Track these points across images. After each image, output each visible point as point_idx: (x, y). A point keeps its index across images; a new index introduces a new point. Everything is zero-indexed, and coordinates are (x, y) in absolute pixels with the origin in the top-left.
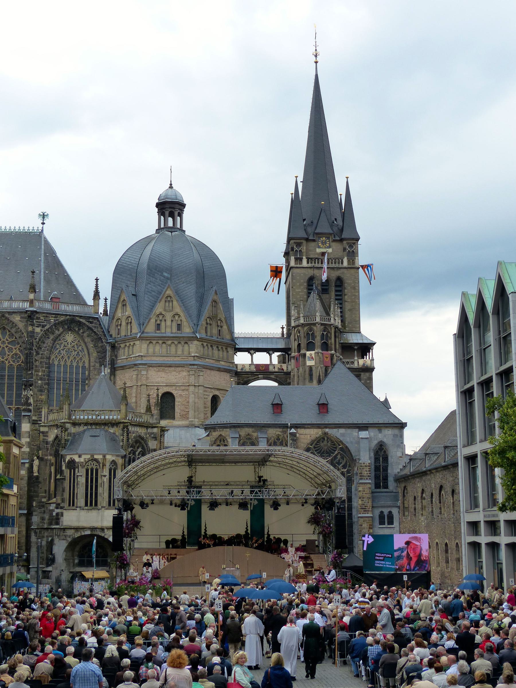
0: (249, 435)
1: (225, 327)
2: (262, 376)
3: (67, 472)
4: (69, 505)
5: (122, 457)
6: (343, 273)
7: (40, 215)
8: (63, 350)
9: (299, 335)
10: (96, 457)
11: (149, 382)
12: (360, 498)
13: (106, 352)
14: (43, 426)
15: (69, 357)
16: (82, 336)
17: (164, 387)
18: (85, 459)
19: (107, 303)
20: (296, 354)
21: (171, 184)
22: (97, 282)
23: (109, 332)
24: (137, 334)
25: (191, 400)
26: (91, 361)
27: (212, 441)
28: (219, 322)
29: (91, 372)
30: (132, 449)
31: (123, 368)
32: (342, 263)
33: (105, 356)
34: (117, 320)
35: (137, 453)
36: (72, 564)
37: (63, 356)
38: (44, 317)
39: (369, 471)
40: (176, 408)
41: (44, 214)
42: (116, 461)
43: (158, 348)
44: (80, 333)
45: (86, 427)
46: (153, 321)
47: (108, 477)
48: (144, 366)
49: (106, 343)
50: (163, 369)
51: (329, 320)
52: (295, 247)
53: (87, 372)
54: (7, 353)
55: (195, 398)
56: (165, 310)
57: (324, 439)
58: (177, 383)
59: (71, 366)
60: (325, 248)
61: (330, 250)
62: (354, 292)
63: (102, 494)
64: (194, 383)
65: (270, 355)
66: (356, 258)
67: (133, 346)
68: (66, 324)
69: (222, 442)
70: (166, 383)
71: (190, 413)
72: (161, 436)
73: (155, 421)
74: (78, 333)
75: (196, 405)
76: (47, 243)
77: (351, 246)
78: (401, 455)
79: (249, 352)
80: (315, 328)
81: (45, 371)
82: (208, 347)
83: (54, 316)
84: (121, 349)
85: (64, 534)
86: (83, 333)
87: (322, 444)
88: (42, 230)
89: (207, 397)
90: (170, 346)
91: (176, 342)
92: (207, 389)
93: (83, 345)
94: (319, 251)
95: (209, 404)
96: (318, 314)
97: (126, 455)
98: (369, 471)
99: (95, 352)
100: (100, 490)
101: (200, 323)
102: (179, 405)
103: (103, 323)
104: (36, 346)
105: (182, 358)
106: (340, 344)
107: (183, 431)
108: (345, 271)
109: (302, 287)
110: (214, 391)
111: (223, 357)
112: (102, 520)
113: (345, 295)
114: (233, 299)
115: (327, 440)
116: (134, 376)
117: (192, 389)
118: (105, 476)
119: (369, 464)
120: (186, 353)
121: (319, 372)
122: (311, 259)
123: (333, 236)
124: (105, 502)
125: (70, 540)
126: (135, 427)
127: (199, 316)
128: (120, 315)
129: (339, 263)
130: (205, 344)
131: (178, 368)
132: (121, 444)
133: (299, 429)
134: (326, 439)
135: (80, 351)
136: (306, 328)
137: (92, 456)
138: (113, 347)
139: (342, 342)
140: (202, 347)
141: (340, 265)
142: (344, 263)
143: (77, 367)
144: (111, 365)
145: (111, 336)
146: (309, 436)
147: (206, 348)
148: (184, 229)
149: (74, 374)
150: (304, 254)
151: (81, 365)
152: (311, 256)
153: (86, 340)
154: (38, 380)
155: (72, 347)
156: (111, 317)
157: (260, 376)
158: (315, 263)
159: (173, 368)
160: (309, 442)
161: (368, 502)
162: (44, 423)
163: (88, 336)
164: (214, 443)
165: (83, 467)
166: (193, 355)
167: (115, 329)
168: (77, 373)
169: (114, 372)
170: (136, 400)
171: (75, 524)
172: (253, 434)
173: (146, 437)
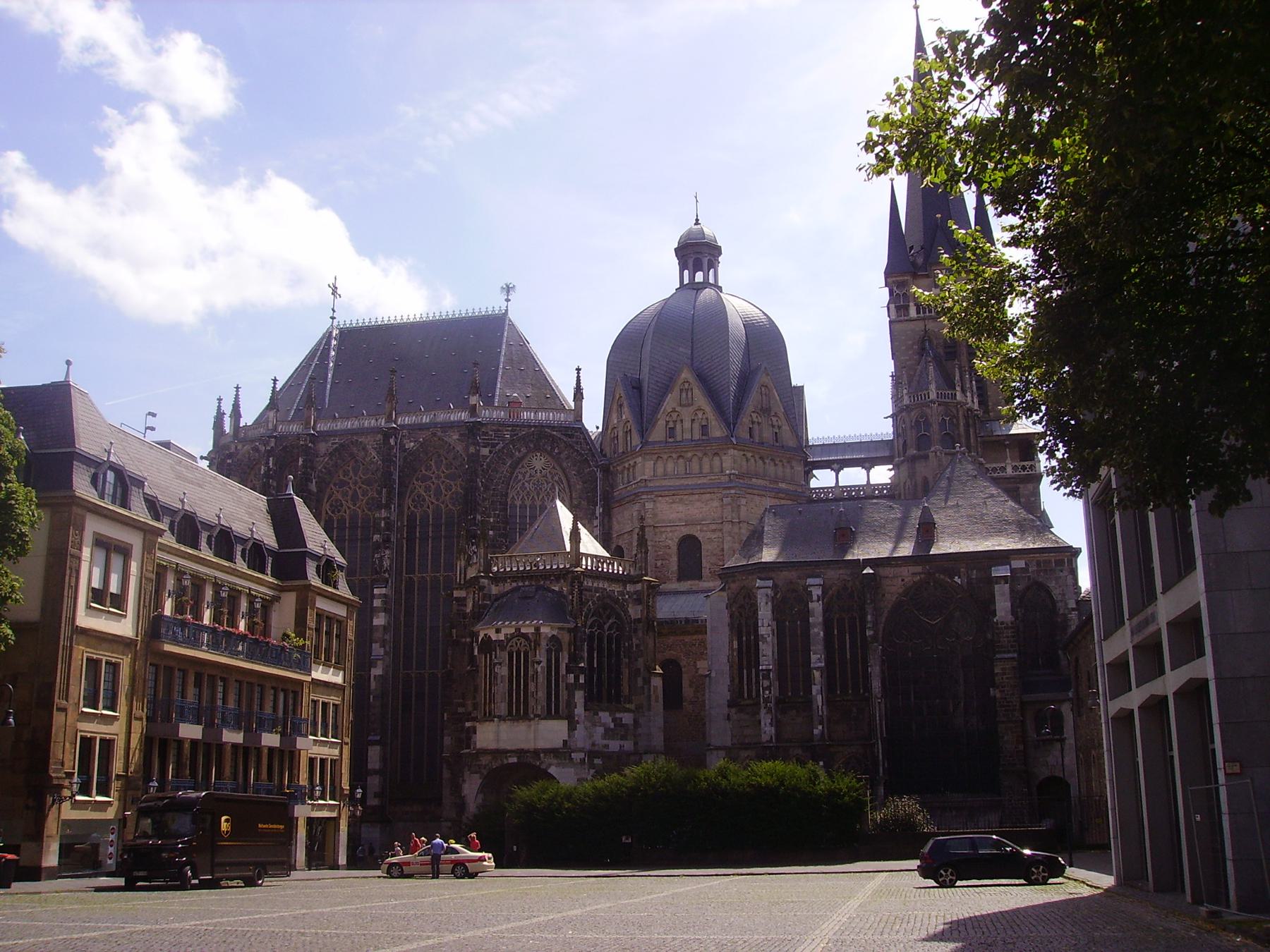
3: (482, 661)
4: (485, 714)
5: (569, 630)
7: (502, 288)
8: (529, 482)
10: (523, 631)
14: (457, 589)
15: (538, 495)
17: (682, 528)
18: (506, 635)
21: (697, 220)
22: (578, 373)
24: (637, 446)
25: (726, 547)
28: (774, 419)
34: (613, 429)
35: (606, 627)
38: (494, 431)
40: (704, 561)
41: (508, 286)
42: (560, 636)
43: (670, 466)
45: (514, 584)
46: (661, 423)
47: (544, 664)
52: (895, 288)
54: (443, 491)
57: (929, 583)
65: (868, 470)
67: (634, 466)
68: (532, 441)
70: (686, 521)
72: (648, 595)
73: (638, 572)
74: (550, 454)
76: (512, 325)
78: (1074, 606)
80: (928, 411)
81: (499, 515)
82: (755, 461)
83: (510, 429)
85: (478, 763)
86: (560, 453)
88: (507, 311)
96: (933, 387)
97: (576, 626)
100: (532, 687)
101: (739, 420)
104: (485, 477)
106: (979, 439)
112: (535, 739)
117: (727, 527)
118: (539, 663)
120: (716, 470)
124: (539, 707)
125: (485, 772)
128: (616, 422)
130: (749, 455)
131: (703, 496)
132: (570, 608)
136: (913, 414)
137: (518, 630)
138: (606, 470)
139: (982, 434)
145: (605, 456)
146: (900, 579)
147: (752, 460)
148: (720, 285)
153: (565, 464)
154: (489, 530)
160: (901, 591)
162: (460, 584)
163: (567, 458)
164: (734, 602)
165: (503, 648)
166: (728, 472)
171: (493, 746)
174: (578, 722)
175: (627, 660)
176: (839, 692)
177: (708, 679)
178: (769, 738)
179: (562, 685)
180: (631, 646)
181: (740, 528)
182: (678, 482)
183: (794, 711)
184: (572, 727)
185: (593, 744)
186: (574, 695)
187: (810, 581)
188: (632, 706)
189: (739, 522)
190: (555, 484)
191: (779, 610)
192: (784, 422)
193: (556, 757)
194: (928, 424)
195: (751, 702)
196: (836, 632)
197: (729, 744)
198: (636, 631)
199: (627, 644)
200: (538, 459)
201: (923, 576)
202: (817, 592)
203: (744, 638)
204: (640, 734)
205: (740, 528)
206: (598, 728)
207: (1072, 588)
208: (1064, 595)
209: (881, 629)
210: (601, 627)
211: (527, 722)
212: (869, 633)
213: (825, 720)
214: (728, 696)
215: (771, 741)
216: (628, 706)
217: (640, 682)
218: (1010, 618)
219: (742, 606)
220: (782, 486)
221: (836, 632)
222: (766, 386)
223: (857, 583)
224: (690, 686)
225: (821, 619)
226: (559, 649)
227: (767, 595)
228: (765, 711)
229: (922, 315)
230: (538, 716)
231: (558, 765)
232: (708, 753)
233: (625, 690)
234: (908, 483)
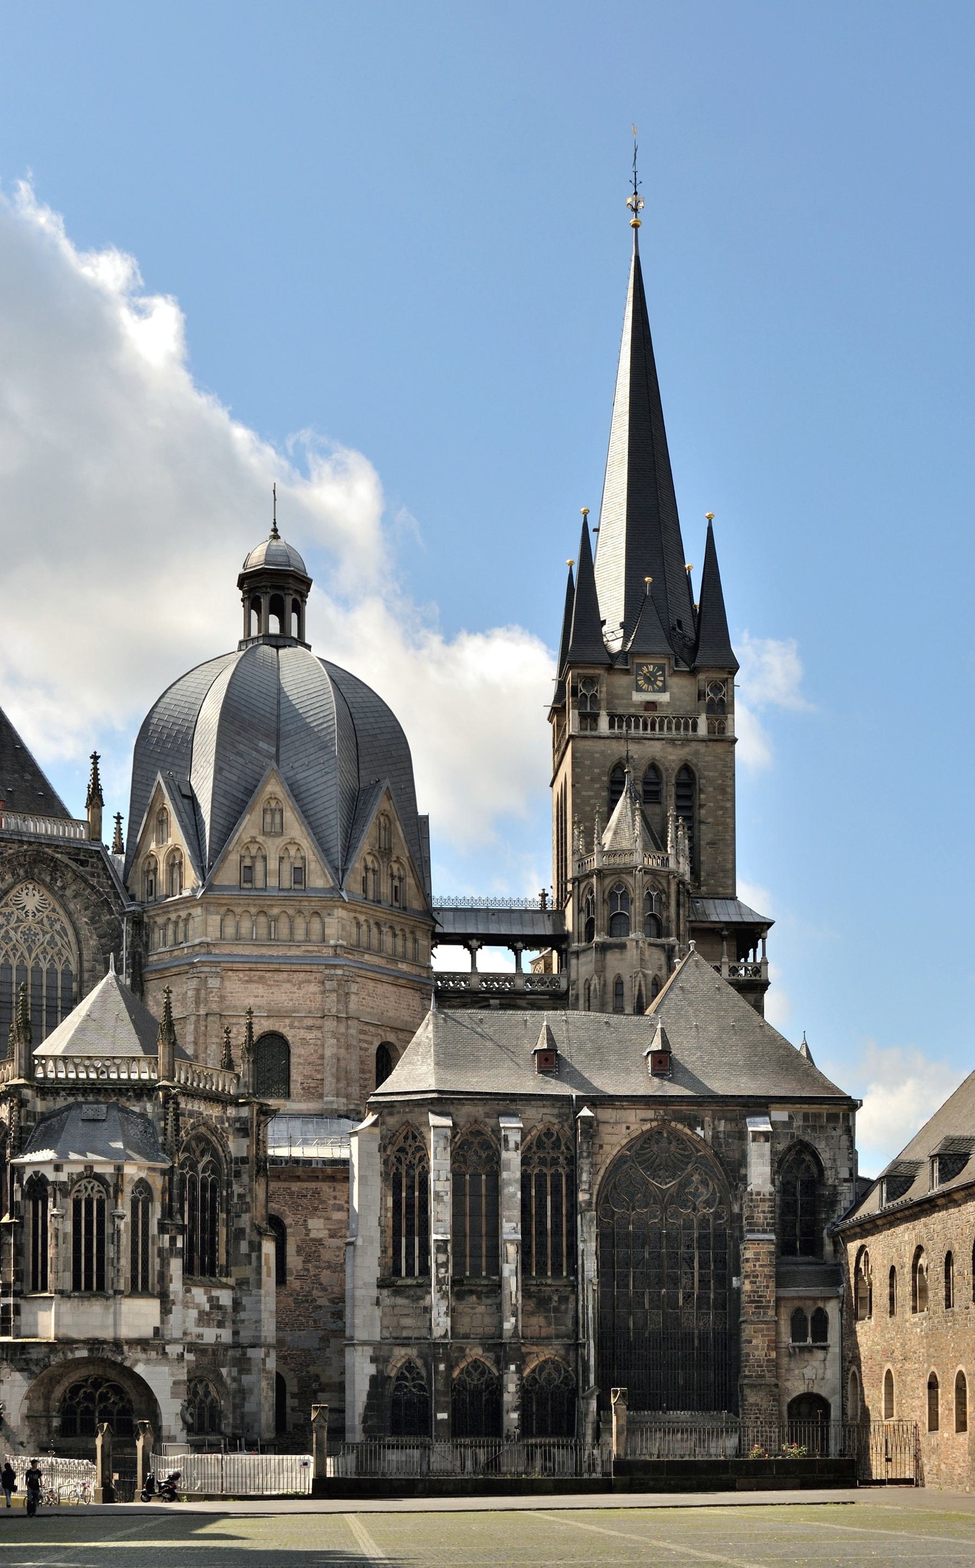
0: (476, 1121)
2: (497, 1002)
6: (696, 753)
8: (15, 929)
9: (590, 897)
11: (227, 1008)
12: (747, 1277)
13: (120, 936)
15: (30, 950)
16: (62, 896)
19: (122, 826)
20: (584, 944)
23: (127, 889)
25: (328, 1053)
26: (85, 957)
27: (386, 1137)
28: (395, 866)
29: (85, 984)
30: (187, 1155)
31: (162, 972)
32: (695, 728)
33: (121, 943)
35: (200, 1166)
36: (44, 1431)
37: (14, 945)
39: (771, 1212)
43: (246, 925)
44: (56, 888)
46: (234, 858)
48: (213, 969)
49: (120, 914)
50: (261, 978)
51: (665, 861)
52: (580, 686)
53: (74, 985)
55: (339, 1047)
56: (263, 835)
57: (660, 1133)
58: (294, 1012)
59: (37, 970)
60: (654, 691)
61: (664, 698)
62: (722, 800)
63: (115, 1261)
64: (334, 1011)
66: (729, 716)
67: (186, 920)
69: (410, 1141)
71: (326, 1082)
72: (258, 1125)
73: (242, 1090)
74: (50, 888)
75: (343, 1063)
77: (716, 688)
78: (847, 1176)
79: (467, 946)
80: (630, 880)
82: (369, 926)
84: (156, 930)
86: (63, 888)
87: (655, 1148)
89: (365, 1045)
90: (276, 919)
91: (291, 912)
92: (366, 1028)
93: (64, 919)
94: (640, 699)
95: (372, 1064)
98: (771, 1212)
99: (95, 937)
102: (299, 1064)
103: (112, 867)
105: (308, 951)
107: (310, 1126)
108: (702, 748)
109: (597, 786)
110: (383, 1034)
111: (405, 953)
113: (701, 806)
114: (427, 817)
115: (668, 1138)
116: (190, 993)
117: (330, 1025)
119: (771, 1194)
121: (640, 986)
122: (620, 717)
123: (673, 662)
126: (196, 1102)
127: (349, 848)
129: (686, 728)
131: (296, 975)
133: (599, 1111)
134: (665, 1135)
135: (58, 933)
136: (607, 881)
138: (138, 923)
140: (354, 922)
141: (691, 733)
142: (699, 729)
143: (52, 972)
144: (133, 968)
145: (132, 898)
146: (624, 1126)
147: (364, 928)
149: (44, 988)
150: (603, 704)
151: (59, 968)
152: (620, 711)
153: (72, 906)
155: (38, 923)
156: (130, 853)
157: (492, 1002)
158: (629, 727)
159: (285, 975)
160: (624, 1142)
161: (767, 1287)
163: (75, 897)
166: (332, 942)
167: (143, 882)
168: (52, 987)
169: (142, 985)
170: (196, 1051)
172: (487, 1120)
173: (222, 1128)
174: (174, 1303)
175: (224, 1216)
176: (534, 1274)
177: (351, 1247)
178: (443, 1333)
179: (153, 1251)
180: (230, 1196)
181: (348, 1027)
182: (256, 951)
183: (474, 1298)
184: (166, 1311)
185: (185, 1334)
186: (168, 1264)
187: (505, 1123)
188: (231, 1281)
189: (347, 1018)
190: (57, 938)
191: (459, 1157)
192: (410, 874)
193: (144, 1350)
194: (626, 899)
195: (415, 1282)
196: (533, 1193)
197: (377, 1337)
198: (238, 1174)
199: (225, 1193)
200: (30, 894)
201: (654, 1124)
202: (514, 1138)
203: (404, 1194)
204: (243, 1321)
205: (348, 1027)
206: (190, 1310)
207: (845, 1152)
208: (835, 1160)
209: (595, 1193)
210: (193, 1167)
211: (104, 1302)
212: (582, 1197)
213: (520, 1311)
214: (377, 1272)
215: (445, 1336)
216: (224, 1280)
217: (244, 1247)
218: (768, 1188)
219: (402, 1150)
220: (403, 967)
221: (533, 1193)
222: (387, 816)
223: (566, 1128)
224: (299, 1251)
225: (518, 1175)
226: (149, 1199)
227: (446, 1137)
228: (439, 1295)
229: (616, 731)
230: (121, 1292)
231: (148, 1362)
232: (347, 1349)
233: (222, 1258)
234: (595, 981)
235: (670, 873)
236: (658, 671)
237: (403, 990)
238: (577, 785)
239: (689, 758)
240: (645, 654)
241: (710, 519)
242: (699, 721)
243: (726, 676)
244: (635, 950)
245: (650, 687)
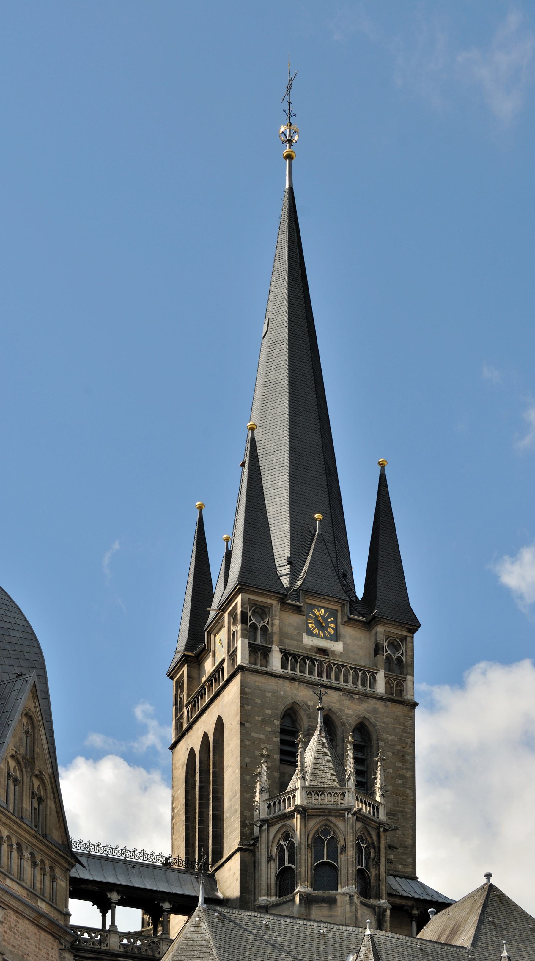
1: (51, 804)
32: (373, 684)
60: (325, 638)
61: (337, 647)
80: (340, 824)
108: (380, 706)
109: (269, 729)
136: (312, 823)
152: (294, 650)
220: (42, 906)
235: (380, 824)
236: (329, 617)
237: (43, 933)
238: (247, 725)
239: (367, 715)
240: (317, 595)
241: (382, 466)
242: (377, 676)
243: (405, 634)
244: (348, 907)
245: (321, 633)
